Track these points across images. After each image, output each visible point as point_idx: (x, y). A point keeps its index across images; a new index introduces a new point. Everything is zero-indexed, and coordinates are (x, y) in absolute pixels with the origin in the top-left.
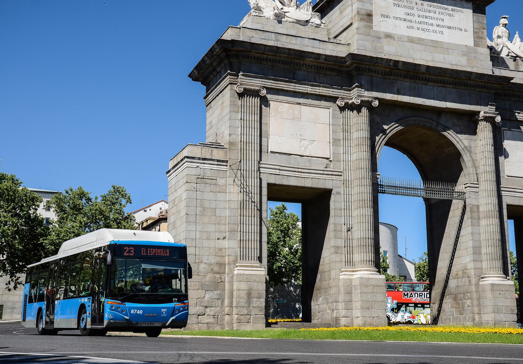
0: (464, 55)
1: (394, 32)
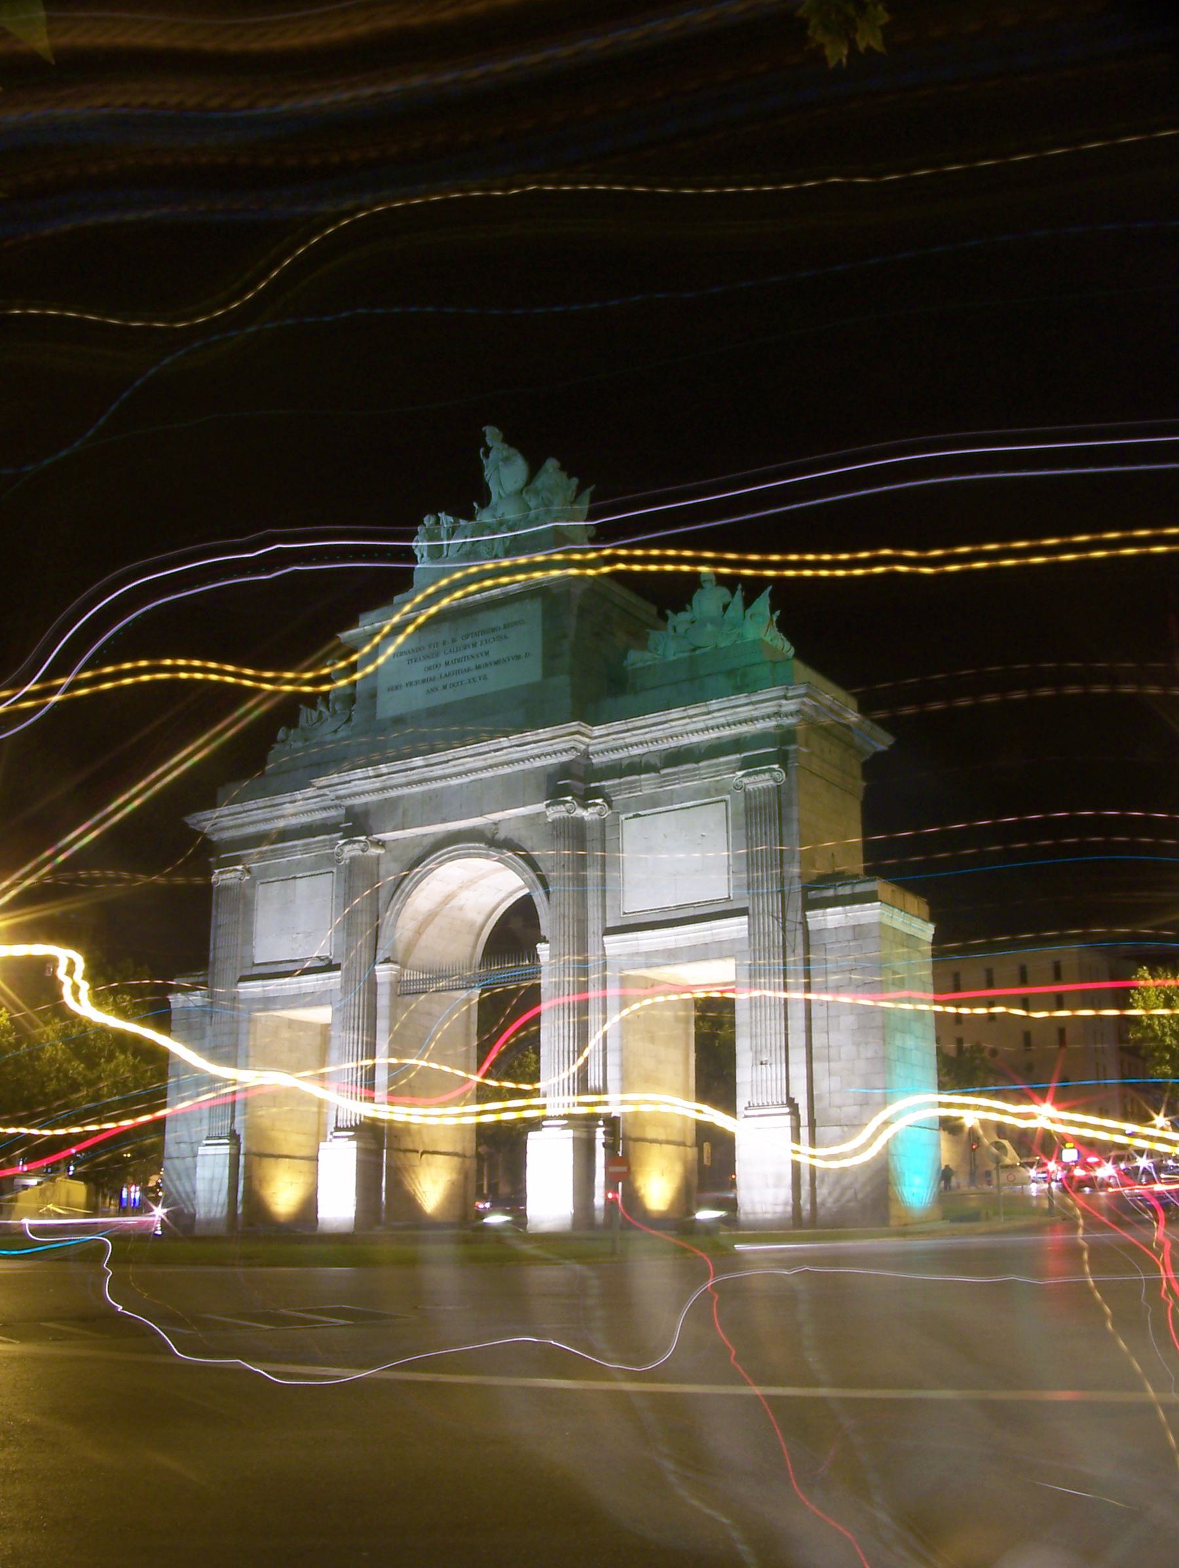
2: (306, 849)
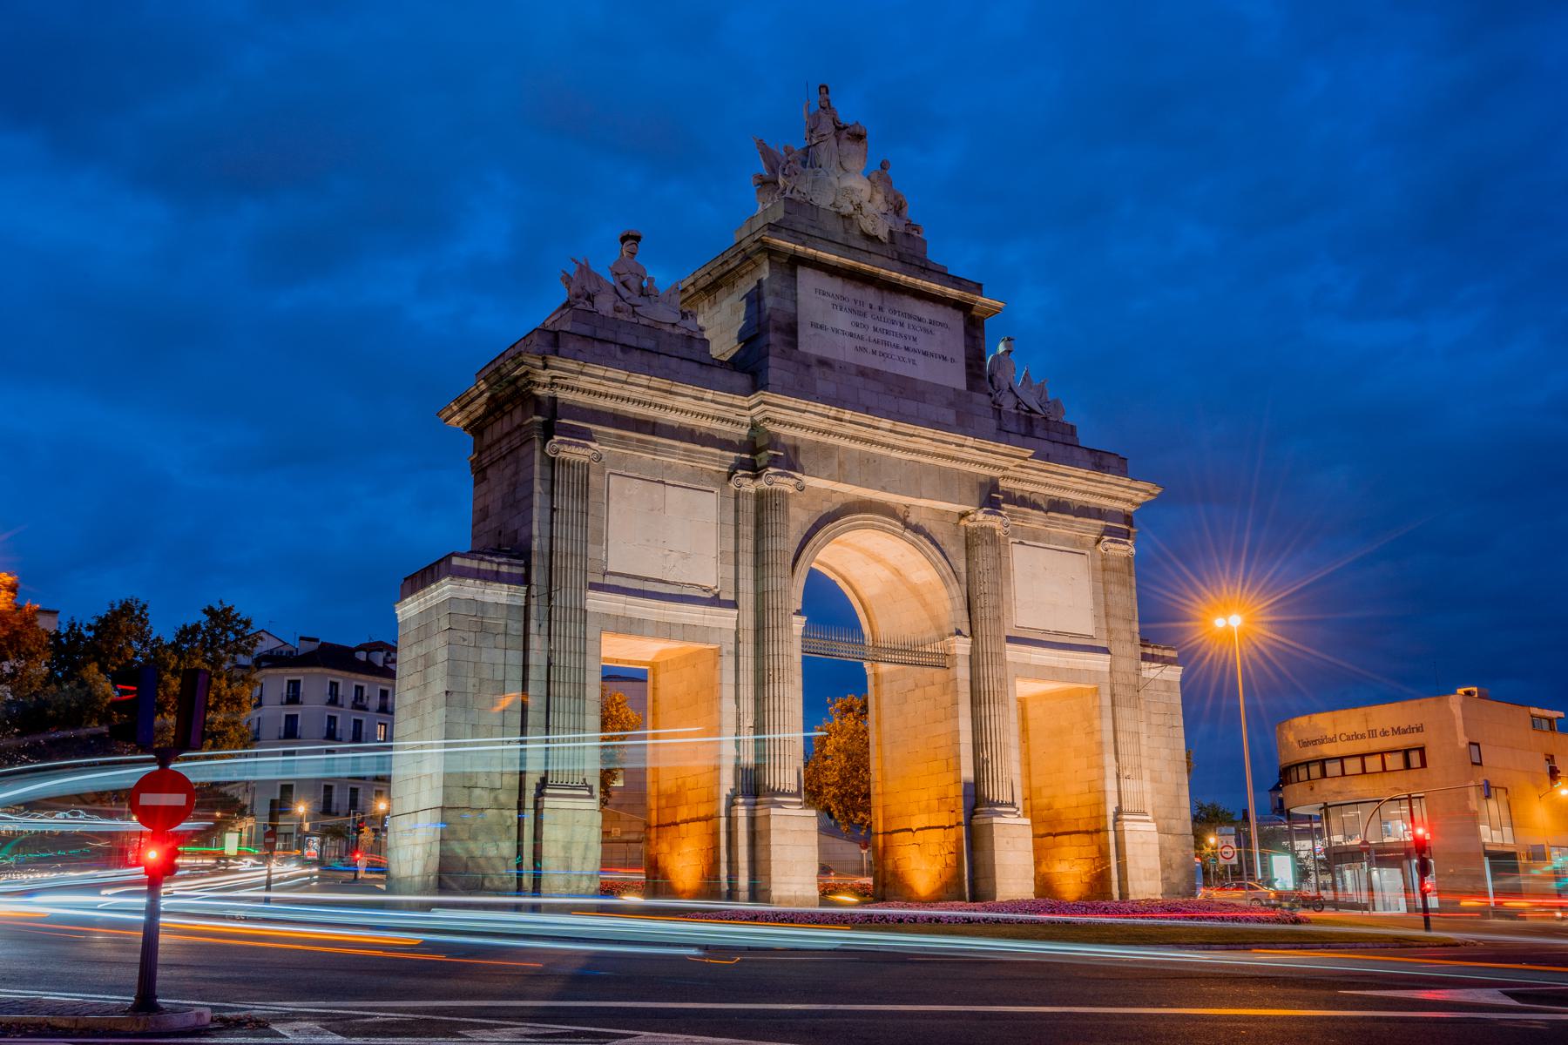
0: (951, 405)
1: (833, 357)
2: (688, 454)
